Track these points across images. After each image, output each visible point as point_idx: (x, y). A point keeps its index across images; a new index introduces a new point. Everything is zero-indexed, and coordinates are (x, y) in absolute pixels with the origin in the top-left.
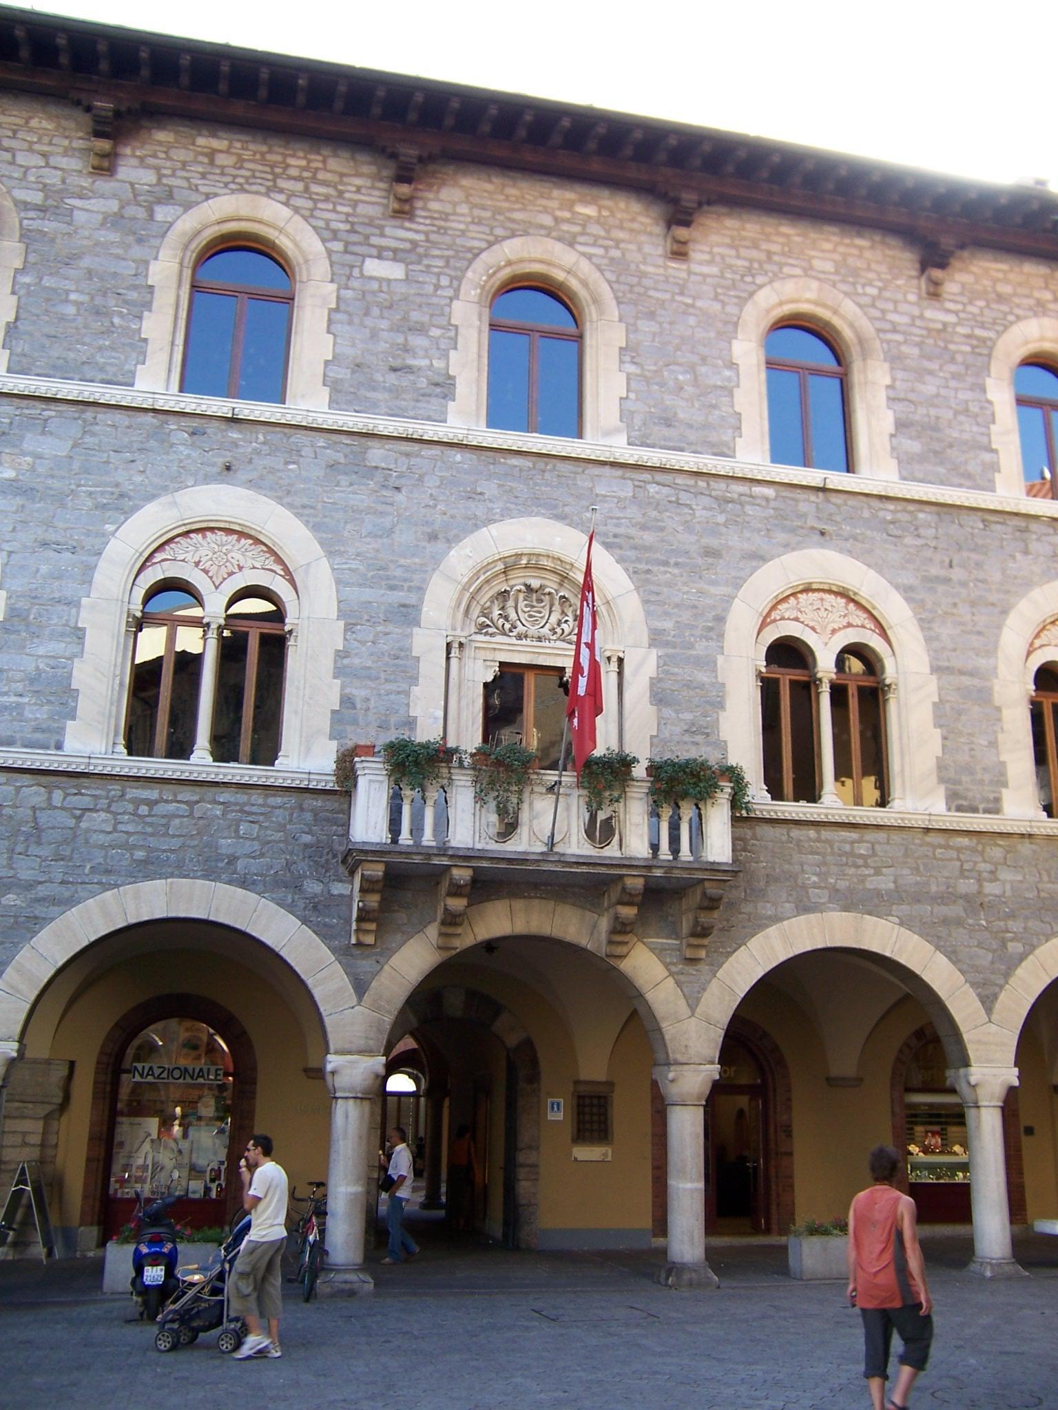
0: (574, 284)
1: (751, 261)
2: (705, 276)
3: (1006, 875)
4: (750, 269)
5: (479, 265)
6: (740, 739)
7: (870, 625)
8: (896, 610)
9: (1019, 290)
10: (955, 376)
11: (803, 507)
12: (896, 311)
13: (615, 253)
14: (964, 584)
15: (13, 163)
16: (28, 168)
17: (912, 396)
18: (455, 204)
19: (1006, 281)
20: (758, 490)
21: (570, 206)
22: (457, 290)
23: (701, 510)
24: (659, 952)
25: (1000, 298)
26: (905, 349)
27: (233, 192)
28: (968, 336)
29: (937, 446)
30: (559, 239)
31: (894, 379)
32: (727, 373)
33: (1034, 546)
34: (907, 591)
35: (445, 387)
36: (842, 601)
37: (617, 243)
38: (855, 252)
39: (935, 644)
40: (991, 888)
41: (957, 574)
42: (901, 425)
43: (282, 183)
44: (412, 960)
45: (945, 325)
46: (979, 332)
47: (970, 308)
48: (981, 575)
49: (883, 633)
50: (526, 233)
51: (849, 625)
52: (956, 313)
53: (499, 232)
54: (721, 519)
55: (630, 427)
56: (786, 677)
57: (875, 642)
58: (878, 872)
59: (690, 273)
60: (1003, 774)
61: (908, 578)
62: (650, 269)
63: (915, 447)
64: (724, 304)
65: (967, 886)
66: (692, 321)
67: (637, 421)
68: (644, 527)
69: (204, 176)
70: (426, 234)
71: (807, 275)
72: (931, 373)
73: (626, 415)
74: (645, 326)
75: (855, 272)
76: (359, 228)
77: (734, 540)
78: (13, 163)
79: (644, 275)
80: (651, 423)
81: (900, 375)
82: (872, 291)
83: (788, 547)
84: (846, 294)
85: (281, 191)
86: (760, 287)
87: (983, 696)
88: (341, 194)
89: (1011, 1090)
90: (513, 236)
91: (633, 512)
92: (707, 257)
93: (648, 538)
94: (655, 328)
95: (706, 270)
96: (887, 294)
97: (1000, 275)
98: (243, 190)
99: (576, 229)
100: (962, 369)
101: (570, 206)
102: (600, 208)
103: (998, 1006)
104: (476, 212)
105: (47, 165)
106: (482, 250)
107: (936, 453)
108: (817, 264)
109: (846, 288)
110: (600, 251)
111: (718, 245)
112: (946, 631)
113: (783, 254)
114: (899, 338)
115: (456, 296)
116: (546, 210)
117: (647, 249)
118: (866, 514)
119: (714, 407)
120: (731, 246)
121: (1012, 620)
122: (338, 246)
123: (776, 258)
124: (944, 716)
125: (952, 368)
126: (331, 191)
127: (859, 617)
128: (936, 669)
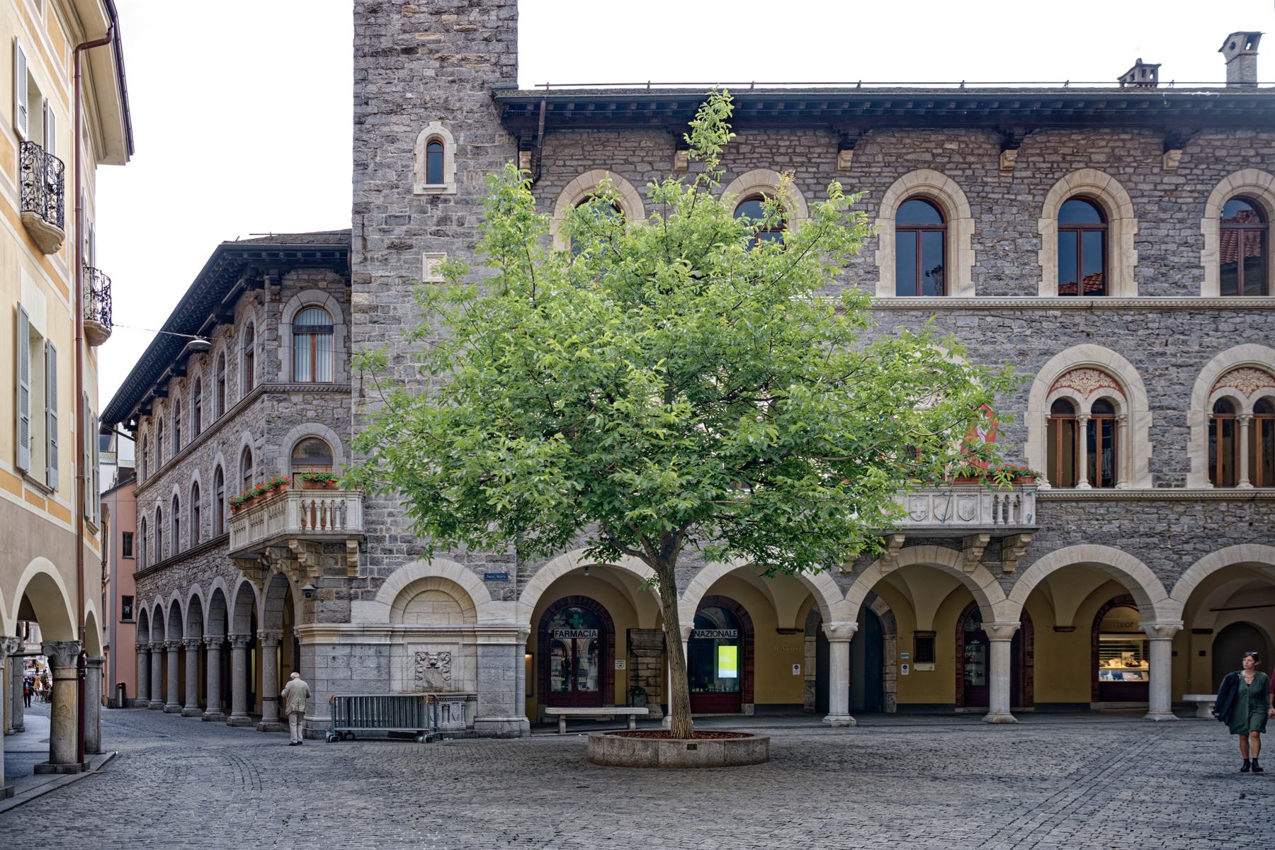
0: (943, 196)
1: (1052, 163)
2: (1023, 178)
3: (1185, 520)
4: (1051, 168)
5: (889, 194)
6: (1035, 455)
7: (1113, 385)
8: (1130, 375)
9: (1232, 152)
10: (1181, 221)
11: (1077, 319)
12: (1144, 182)
13: (969, 172)
14: (1174, 355)
15: (635, 171)
16: (643, 173)
17: (1150, 239)
18: (874, 155)
19: (1223, 147)
20: (1050, 313)
21: (940, 145)
22: (878, 212)
23: (1017, 327)
24: (990, 569)
25: (1218, 160)
26: (1149, 207)
27: (751, 169)
28: (1191, 192)
29: (1163, 270)
30: (935, 169)
31: (1140, 229)
32: (1035, 241)
33: (1222, 326)
34: (1138, 364)
35: (873, 273)
36: (1096, 373)
37: (970, 164)
38: (1121, 144)
39: (1153, 393)
40: (1175, 529)
41: (1171, 349)
42: (1142, 258)
43: (777, 159)
44: (870, 578)
45: (1177, 185)
46: (1199, 187)
47: (1195, 171)
48: (1186, 349)
49: (1121, 390)
50: (916, 168)
51: (1101, 386)
52: (1185, 176)
53: (900, 170)
54: (1028, 332)
55: (977, 285)
56: (1062, 417)
57: (1116, 395)
58: (1110, 522)
59: (1013, 178)
60: (1188, 465)
61: (1139, 355)
62: (989, 180)
63: (1149, 272)
64: (1034, 196)
65: (1161, 527)
66: (1014, 210)
67: (981, 279)
68: (984, 343)
69: (734, 161)
70: (859, 178)
71: (1087, 167)
72: (1163, 221)
73: (975, 276)
74: (987, 217)
75: (1119, 159)
76: (821, 181)
77: (1037, 344)
78: (635, 171)
79: (986, 184)
80: (988, 279)
81: (1144, 225)
82: (1131, 170)
83: (1067, 345)
84: (1112, 175)
85: (777, 164)
86: (1057, 180)
87: (1181, 422)
88: (810, 159)
89: (1178, 632)
90: (909, 171)
91: (978, 334)
92: (1025, 165)
93: (987, 348)
94: (993, 218)
95: (1024, 174)
96: (1140, 171)
97: (1218, 143)
98: (756, 167)
99: (946, 160)
100: (1185, 215)
101: (940, 145)
102: (960, 142)
103: (1175, 589)
104: (887, 158)
106: (891, 184)
107: (1163, 275)
108: (1095, 157)
109: (1112, 171)
110: (960, 173)
111: (1033, 155)
112: (1160, 385)
113: (1073, 154)
114: (1145, 200)
115: (877, 216)
116: (927, 150)
117: (988, 166)
118: (1116, 318)
119: (1025, 264)
120: (1039, 155)
121: (1203, 374)
122: (810, 194)
123: (1068, 158)
124: (1156, 435)
125: (1179, 215)
126: (804, 159)
127: (1106, 382)
128: (1152, 408)
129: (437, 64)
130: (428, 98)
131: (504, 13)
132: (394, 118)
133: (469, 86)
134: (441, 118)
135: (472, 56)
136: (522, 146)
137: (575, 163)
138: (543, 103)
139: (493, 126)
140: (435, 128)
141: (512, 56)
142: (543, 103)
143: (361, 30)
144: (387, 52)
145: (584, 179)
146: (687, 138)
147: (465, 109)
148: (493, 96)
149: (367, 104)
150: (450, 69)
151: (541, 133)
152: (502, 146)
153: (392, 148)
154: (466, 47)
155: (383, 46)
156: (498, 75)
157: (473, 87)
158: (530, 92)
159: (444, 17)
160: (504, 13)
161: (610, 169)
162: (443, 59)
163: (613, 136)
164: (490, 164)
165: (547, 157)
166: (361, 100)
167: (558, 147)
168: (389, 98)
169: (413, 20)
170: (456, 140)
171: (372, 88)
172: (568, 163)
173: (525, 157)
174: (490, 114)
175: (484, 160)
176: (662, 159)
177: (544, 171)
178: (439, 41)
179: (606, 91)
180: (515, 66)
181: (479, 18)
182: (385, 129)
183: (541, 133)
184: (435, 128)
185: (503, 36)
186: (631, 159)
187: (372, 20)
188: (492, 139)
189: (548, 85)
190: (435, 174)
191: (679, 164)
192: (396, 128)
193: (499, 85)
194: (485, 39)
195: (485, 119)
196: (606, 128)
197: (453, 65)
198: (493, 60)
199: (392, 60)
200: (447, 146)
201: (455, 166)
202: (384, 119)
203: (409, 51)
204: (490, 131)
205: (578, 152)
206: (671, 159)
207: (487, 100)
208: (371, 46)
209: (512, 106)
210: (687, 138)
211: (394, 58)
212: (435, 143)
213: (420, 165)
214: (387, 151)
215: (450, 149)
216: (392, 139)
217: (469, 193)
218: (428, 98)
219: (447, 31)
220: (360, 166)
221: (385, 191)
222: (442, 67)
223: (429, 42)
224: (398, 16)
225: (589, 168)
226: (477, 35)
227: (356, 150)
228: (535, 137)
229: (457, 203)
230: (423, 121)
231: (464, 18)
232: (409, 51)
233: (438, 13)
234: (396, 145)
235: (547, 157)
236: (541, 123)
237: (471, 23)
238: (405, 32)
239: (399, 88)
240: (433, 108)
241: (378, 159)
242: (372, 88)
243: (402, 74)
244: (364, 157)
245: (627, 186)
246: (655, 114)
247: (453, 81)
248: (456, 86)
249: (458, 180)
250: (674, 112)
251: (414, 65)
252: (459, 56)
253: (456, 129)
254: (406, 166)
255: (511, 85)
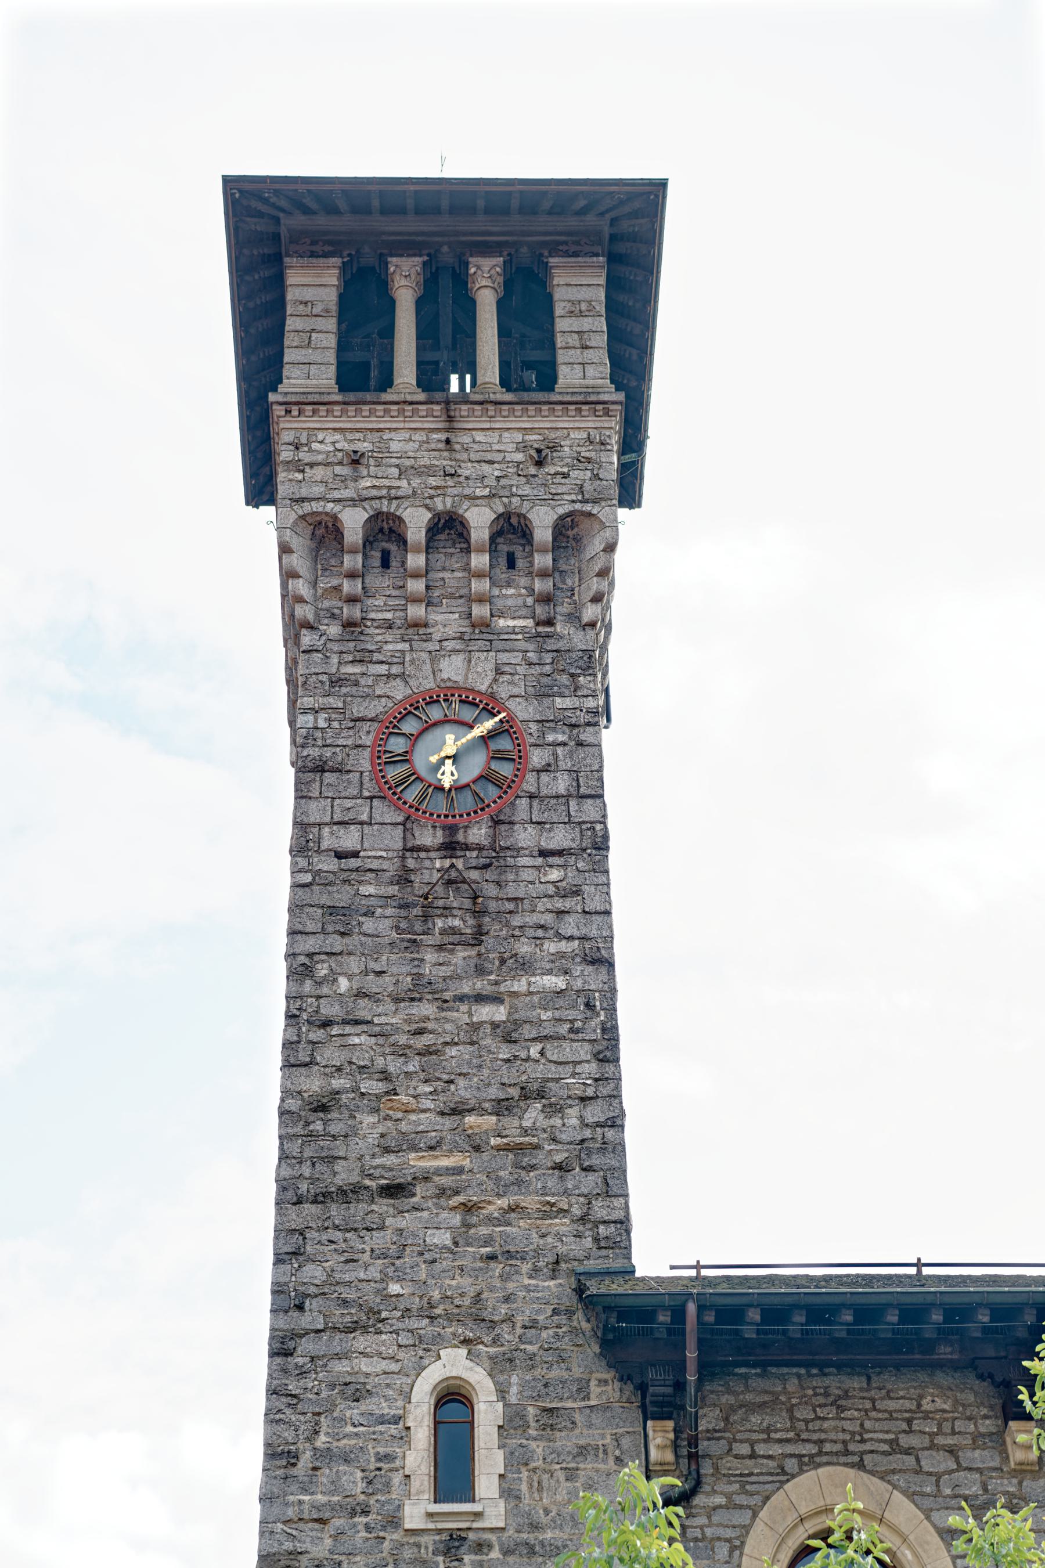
15: (918, 1471)
16: (938, 1476)
78: (918, 1471)
105: (960, 1467)
129: (457, 1219)
130: (436, 1295)
131: (595, 1113)
132: (361, 1342)
133: (526, 1267)
134: (466, 1342)
135: (530, 1202)
136: (656, 1407)
137: (776, 1450)
138: (691, 1308)
139: (584, 1361)
140: (454, 1363)
141: (617, 1203)
142: (691, 1308)
143: (294, 1148)
144: (347, 1194)
145: (804, 1490)
146: (1024, 1396)
147: (519, 1319)
148: (579, 1289)
149: (300, 1308)
150: (484, 1231)
151: (691, 1378)
152: (605, 1408)
153: (354, 1412)
154: (518, 1183)
155: (339, 1181)
156: (588, 1242)
157: (536, 1269)
158: (660, 1280)
159: (470, 1120)
160: (595, 1113)
161: (860, 1466)
162: (468, 1208)
163: (856, 1383)
164: (582, 1451)
165: (712, 1435)
166: (288, 1300)
167: (733, 1409)
168: (350, 1295)
169: (404, 1126)
170: (502, 1393)
171: (313, 1273)
172: (761, 1449)
173: (660, 1436)
174: (574, 1331)
175: (566, 1441)
176: (977, 1440)
177: (707, 1469)
178: (459, 1171)
179: (828, 1279)
180: (624, 1224)
181: (542, 1122)
182: (341, 1367)
183: (691, 1378)
184: (454, 1363)
185: (595, 1160)
186: (905, 1441)
187: (318, 1126)
188: (583, 1392)
189: (698, 1267)
190: (453, 1476)
191: (1017, 1456)
192: (364, 1365)
193: (591, 1265)
194: (558, 1167)
195: (565, 1343)
196: (840, 1366)
197: (490, 1221)
198: (577, 1211)
199: (359, 1210)
200: (482, 1408)
201: (499, 1456)
202: (338, 1343)
203: (394, 1191)
204: (577, 1372)
205: (781, 1421)
206: (998, 1441)
207: (569, 1299)
208: (313, 1180)
209: (624, 1314)
210: (1024, 1396)
211: (363, 1207)
212: (453, 1399)
213: (418, 1457)
214: (342, 1420)
215: (488, 1414)
216: (357, 1392)
217: (535, 1527)
218: (436, 1295)
219: (477, 1148)
220: (280, 1457)
221: (337, 1522)
222: (468, 1226)
223: (438, 1172)
224: (372, 1119)
225: (808, 1463)
226: (540, 1158)
227: (272, 1418)
228: (680, 1386)
229: (507, 1552)
230: (427, 1348)
231: (511, 1123)
232: (394, 1191)
233: (457, 1111)
234: (364, 1406)
235: (712, 1435)
236: (691, 1355)
237: (525, 1132)
238: (387, 1150)
239: (374, 1273)
240: (449, 1318)
241: (322, 1440)
242: (313, 1273)
243: (379, 1240)
244: (289, 1435)
245: (903, 1511)
246: (943, 1334)
247: (492, 1257)
248: (497, 1268)
249: (508, 1493)
250: (986, 1330)
251: (405, 1221)
252: (503, 1203)
253: (500, 1366)
254: (388, 1458)
255: (618, 1264)
